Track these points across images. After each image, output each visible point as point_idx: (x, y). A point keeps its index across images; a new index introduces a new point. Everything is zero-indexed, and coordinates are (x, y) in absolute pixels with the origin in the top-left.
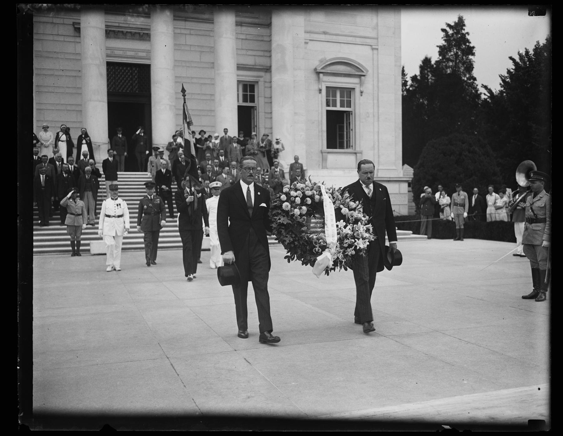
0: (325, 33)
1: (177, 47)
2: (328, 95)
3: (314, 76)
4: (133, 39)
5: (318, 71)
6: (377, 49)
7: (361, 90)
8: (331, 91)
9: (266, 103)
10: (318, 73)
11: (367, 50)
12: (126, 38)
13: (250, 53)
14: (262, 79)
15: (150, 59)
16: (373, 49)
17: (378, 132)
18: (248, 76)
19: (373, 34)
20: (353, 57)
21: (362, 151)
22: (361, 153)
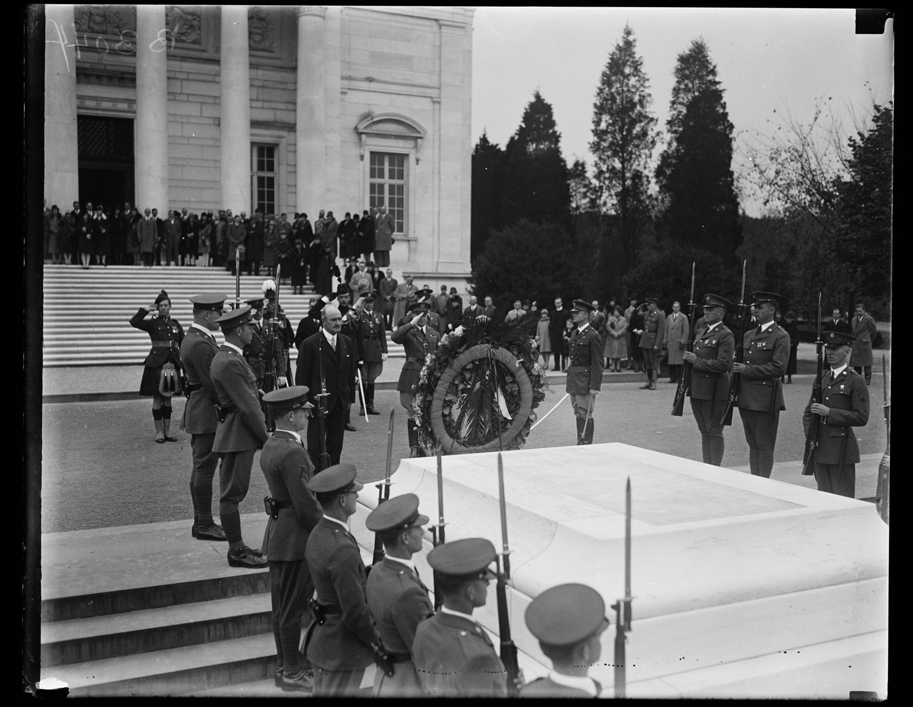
0: (370, 80)
1: (171, 96)
2: (372, 162)
3: (355, 138)
4: (110, 85)
5: (360, 131)
6: (439, 103)
7: (416, 157)
8: (377, 157)
9: (289, 172)
10: (360, 134)
11: (426, 104)
12: (101, 84)
13: (266, 105)
14: (283, 141)
15: (135, 112)
16: (434, 102)
17: (439, 213)
18: (266, 136)
19: (435, 83)
20: (407, 114)
21: (417, 238)
22: (416, 241)
